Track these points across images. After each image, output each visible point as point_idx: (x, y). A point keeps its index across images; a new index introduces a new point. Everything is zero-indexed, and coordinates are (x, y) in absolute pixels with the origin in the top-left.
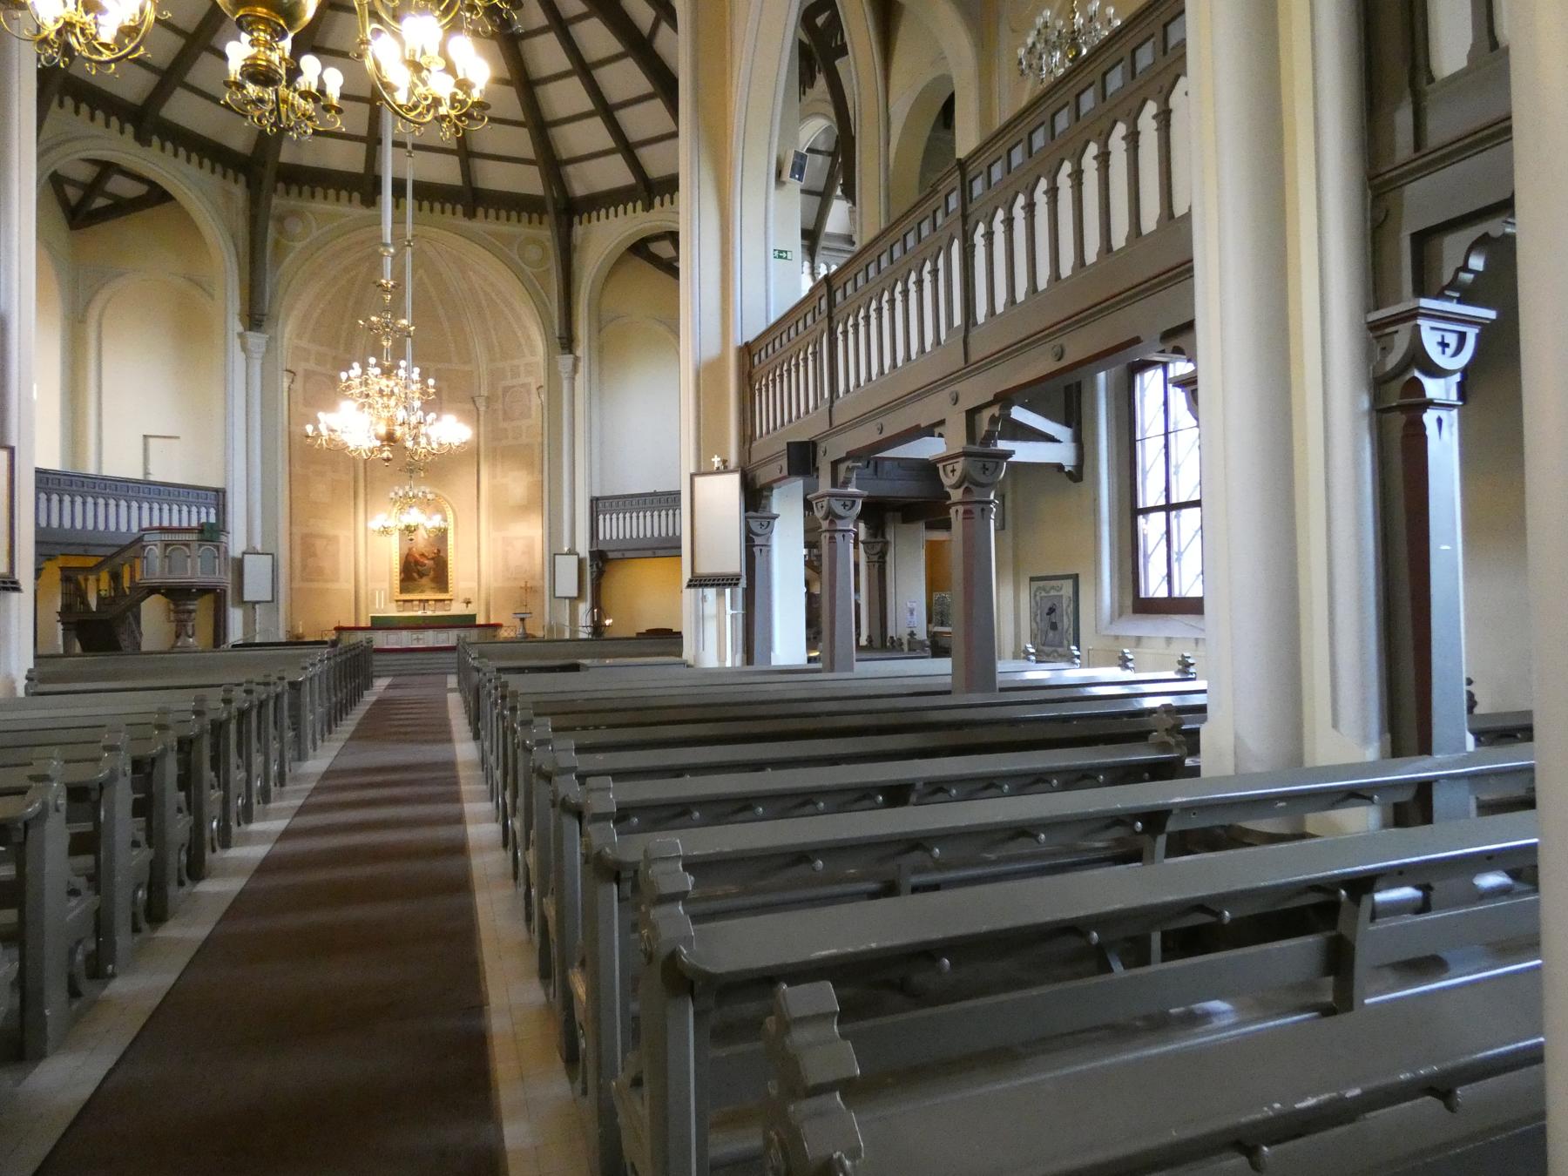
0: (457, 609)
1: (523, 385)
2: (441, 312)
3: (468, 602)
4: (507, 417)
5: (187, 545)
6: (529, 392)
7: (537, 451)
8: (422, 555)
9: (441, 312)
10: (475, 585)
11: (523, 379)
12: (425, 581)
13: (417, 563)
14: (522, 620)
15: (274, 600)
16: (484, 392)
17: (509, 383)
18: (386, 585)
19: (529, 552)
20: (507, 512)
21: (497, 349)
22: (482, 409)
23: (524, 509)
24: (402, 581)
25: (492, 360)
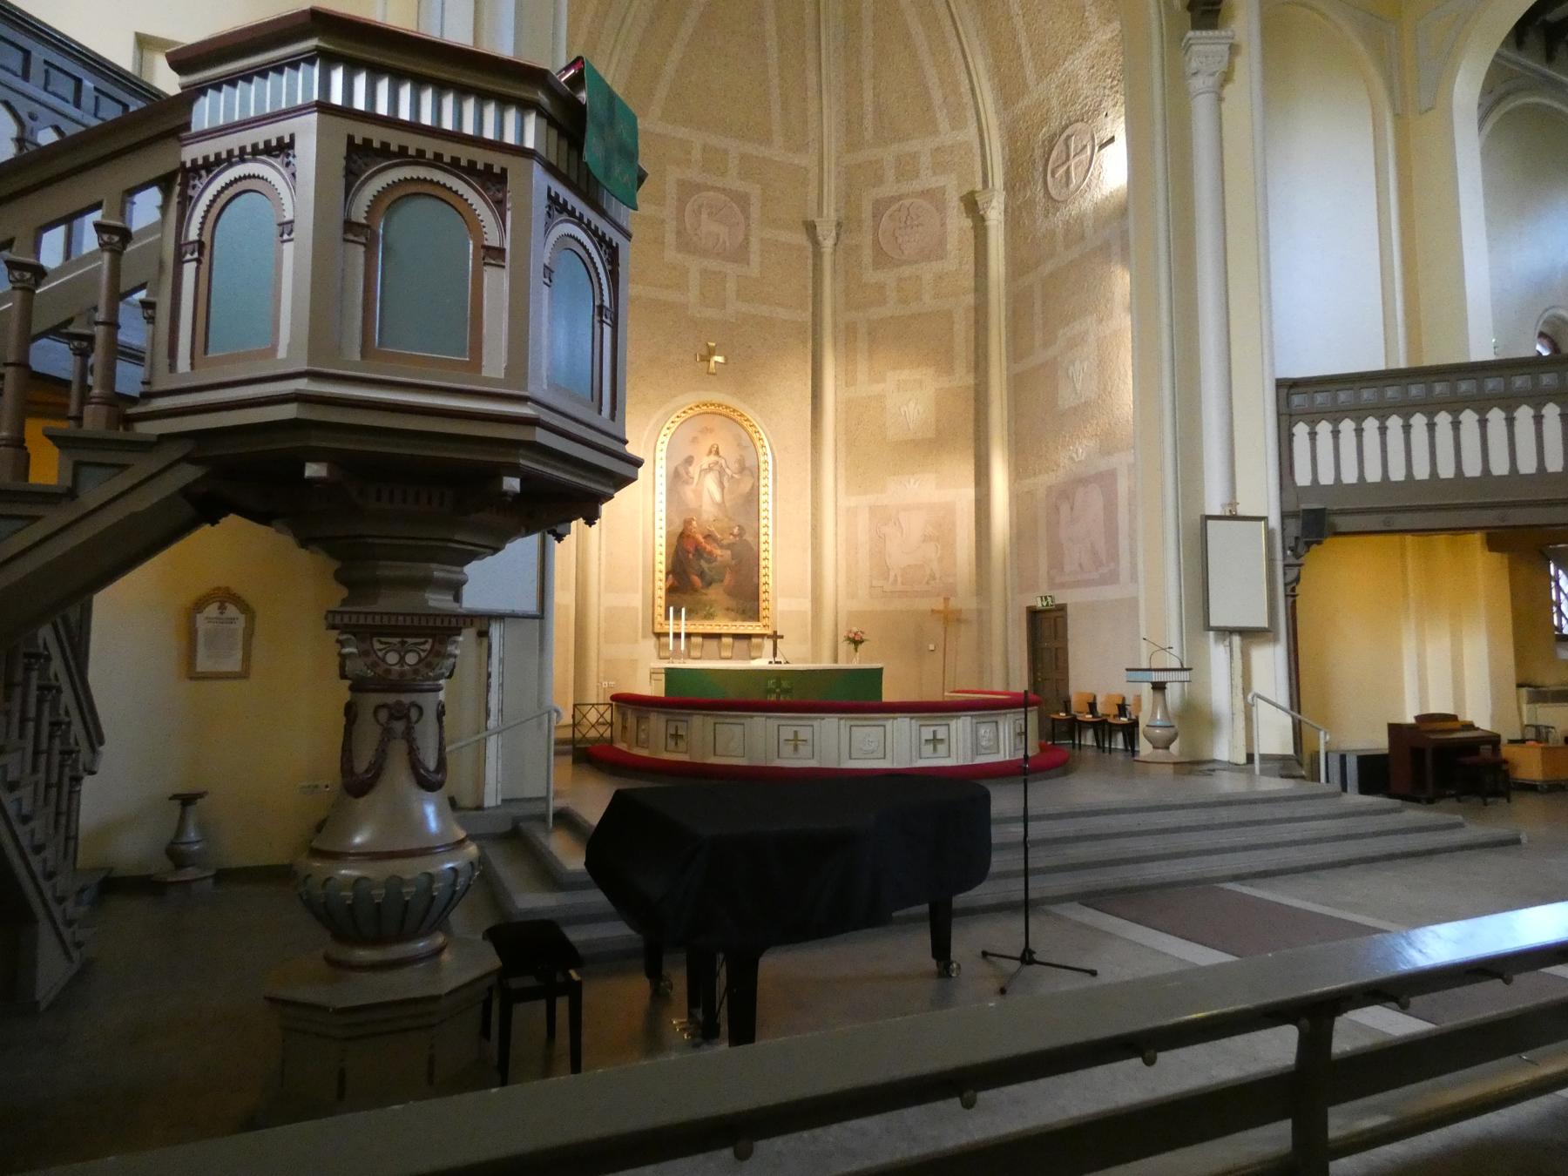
0: (796, 655)
1: (924, 194)
2: (771, 27)
3: (856, 642)
4: (882, 258)
5: (492, 181)
6: (941, 207)
7: (962, 329)
8: (708, 536)
9: (771, 27)
10: (807, 605)
11: (928, 181)
12: (715, 594)
13: (699, 551)
14: (1159, 687)
15: (541, 614)
16: (831, 211)
17: (888, 189)
18: (636, 601)
19: (941, 535)
20: (880, 452)
21: (868, 122)
22: (828, 244)
23: (925, 448)
24: (671, 590)
25: (853, 142)
